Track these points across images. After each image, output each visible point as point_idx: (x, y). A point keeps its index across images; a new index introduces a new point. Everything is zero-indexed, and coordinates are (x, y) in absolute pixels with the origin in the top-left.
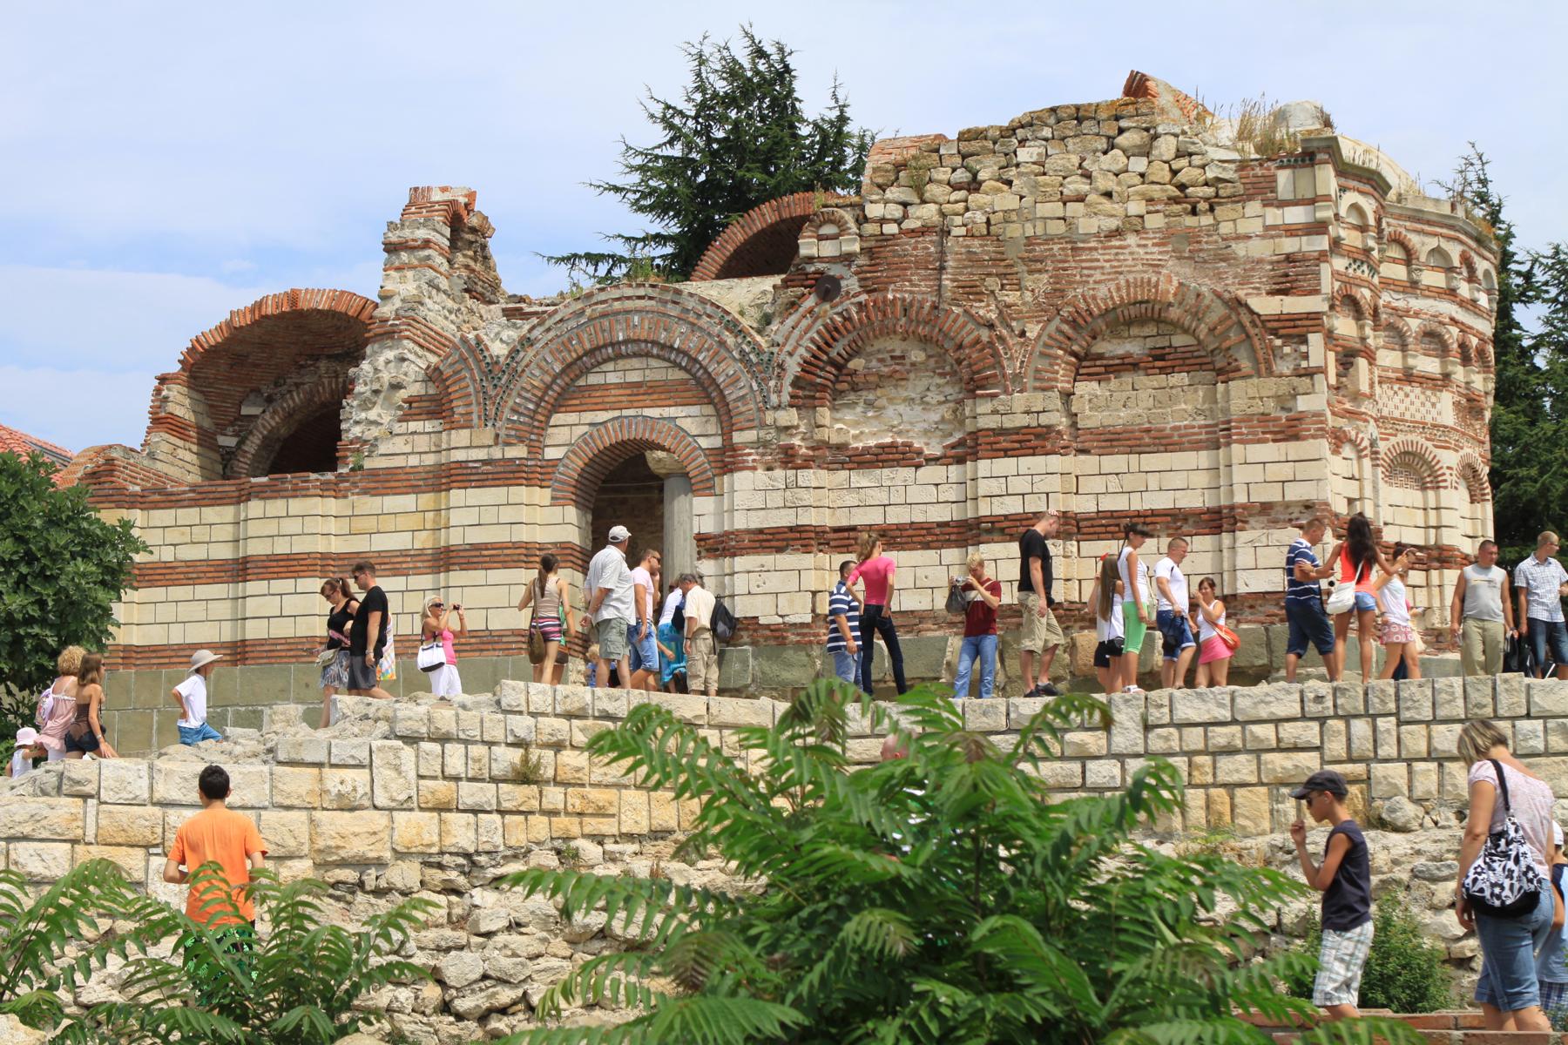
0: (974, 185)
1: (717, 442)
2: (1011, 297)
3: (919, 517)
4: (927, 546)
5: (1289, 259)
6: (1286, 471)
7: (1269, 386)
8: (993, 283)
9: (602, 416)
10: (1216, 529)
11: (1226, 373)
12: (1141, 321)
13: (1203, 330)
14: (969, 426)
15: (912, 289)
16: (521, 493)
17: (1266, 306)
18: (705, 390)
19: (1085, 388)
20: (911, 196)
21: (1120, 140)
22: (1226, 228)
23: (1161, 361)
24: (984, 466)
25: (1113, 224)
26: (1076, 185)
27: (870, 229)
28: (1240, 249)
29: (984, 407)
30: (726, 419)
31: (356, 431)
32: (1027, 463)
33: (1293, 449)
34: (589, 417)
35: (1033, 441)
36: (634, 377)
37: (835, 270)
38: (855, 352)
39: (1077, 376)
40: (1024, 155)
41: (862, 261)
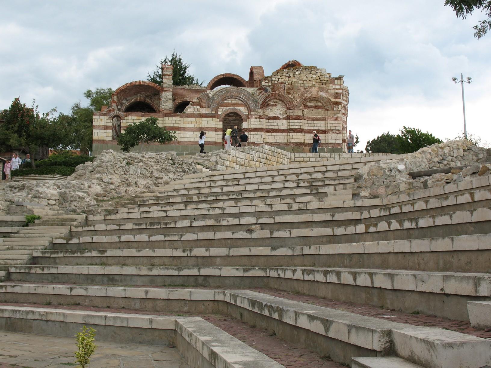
0: (289, 77)
2: (295, 95)
3: (280, 128)
4: (281, 133)
5: (336, 93)
7: (333, 112)
8: (292, 92)
9: (228, 108)
10: (325, 133)
11: (327, 110)
12: (314, 100)
13: (323, 103)
14: (288, 114)
15: (280, 92)
16: (214, 119)
18: (246, 105)
19: (306, 110)
20: (279, 77)
21: (312, 72)
22: (327, 88)
23: (316, 107)
24: (291, 121)
25: (311, 85)
26: (305, 79)
27: (273, 82)
28: (329, 91)
29: (291, 111)
30: (249, 110)
31: (163, 107)
32: (297, 121)
33: (337, 122)
34: (225, 108)
35: (298, 118)
36: (233, 102)
37: (268, 88)
38: (270, 101)
39: (304, 108)
40: (297, 73)
41: (272, 87)
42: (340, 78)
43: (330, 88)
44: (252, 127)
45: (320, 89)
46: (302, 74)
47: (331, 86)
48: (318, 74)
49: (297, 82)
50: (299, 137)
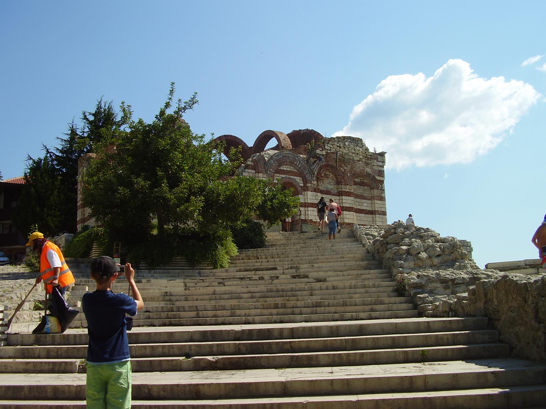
1: (302, 185)
2: (345, 168)
5: (380, 171)
6: (381, 206)
9: (284, 176)
10: (372, 214)
15: (332, 163)
17: (378, 178)
26: (353, 151)
30: (305, 181)
34: (281, 175)
35: (348, 194)
36: (288, 169)
37: (321, 157)
40: (347, 143)
42: (382, 154)
45: (367, 164)
47: (375, 163)
48: (364, 148)
49: (347, 154)
50: (352, 217)
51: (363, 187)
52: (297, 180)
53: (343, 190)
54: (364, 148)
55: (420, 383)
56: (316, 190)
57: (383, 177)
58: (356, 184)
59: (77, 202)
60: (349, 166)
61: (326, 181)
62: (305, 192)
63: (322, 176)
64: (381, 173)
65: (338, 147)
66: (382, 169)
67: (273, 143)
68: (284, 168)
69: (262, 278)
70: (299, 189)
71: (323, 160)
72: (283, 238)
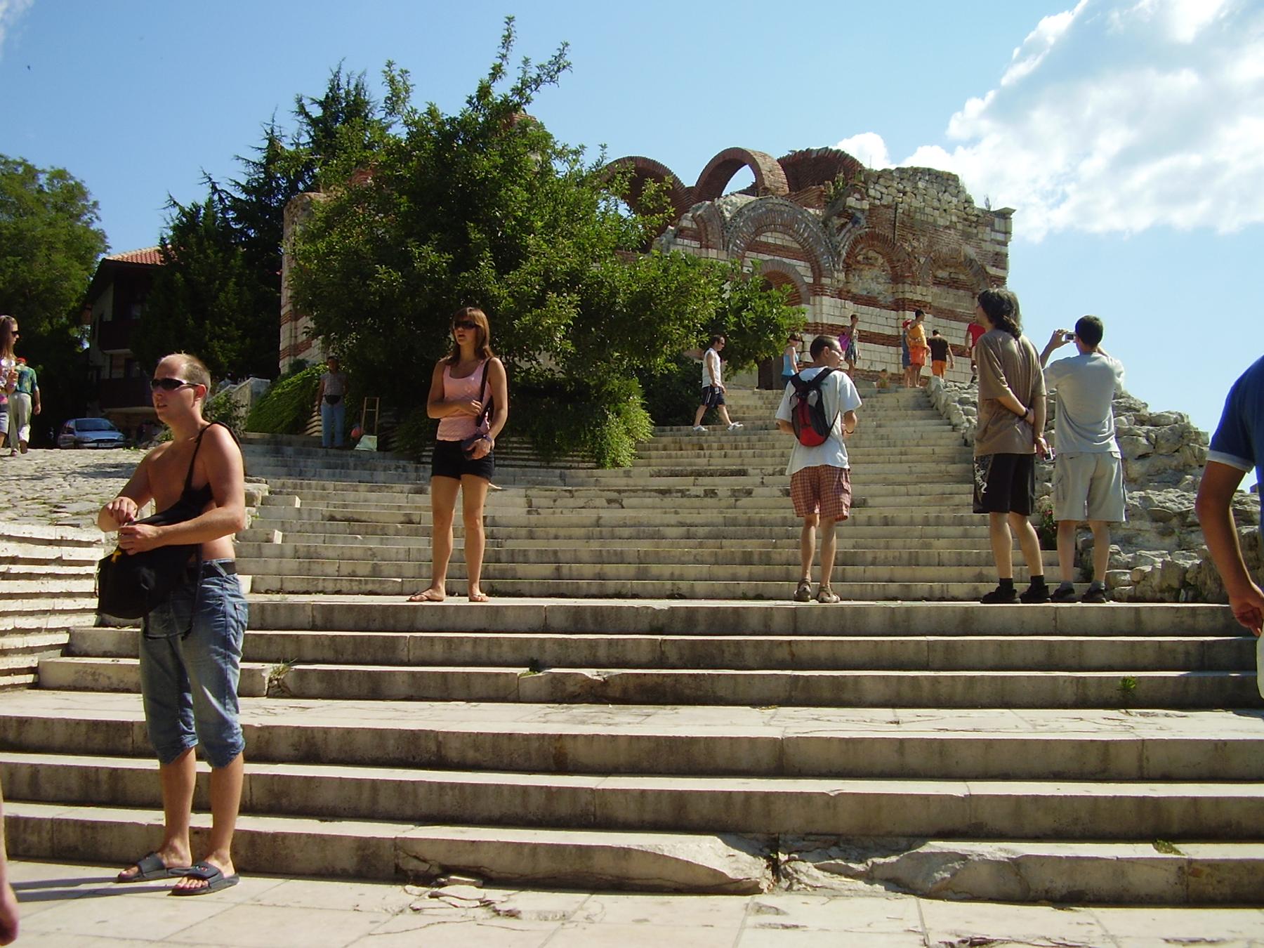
1: (811, 281)
2: (915, 244)
5: (997, 254)
8: (910, 237)
9: (767, 257)
17: (992, 271)
18: (807, 254)
26: (936, 204)
28: (983, 244)
30: (818, 272)
34: (761, 256)
36: (779, 242)
37: (859, 215)
40: (921, 185)
42: (1005, 214)
43: (987, 237)
44: (825, 321)
45: (967, 236)
46: (933, 192)
47: (987, 233)
48: (962, 197)
49: (922, 211)
51: (955, 291)
52: (799, 269)
53: (908, 296)
54: (962, 197)
55: (1128, 762)
56: (841, 294)
57: (1005, 268)
58: (938, 282)
59: (279, 307)
60: (924, 240)
61: (868, 274)
62: (818, 298)
63: (859, 262)
64: (1000, 260)
65: (899, 191)
66: (1003, 249)
67: (743, 178)
68: (769, 238)
69: (711, 493)
70: (803, 289)
71: (863, 222)
72: (760, 403)
